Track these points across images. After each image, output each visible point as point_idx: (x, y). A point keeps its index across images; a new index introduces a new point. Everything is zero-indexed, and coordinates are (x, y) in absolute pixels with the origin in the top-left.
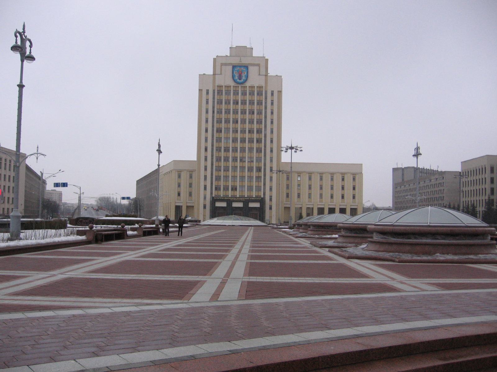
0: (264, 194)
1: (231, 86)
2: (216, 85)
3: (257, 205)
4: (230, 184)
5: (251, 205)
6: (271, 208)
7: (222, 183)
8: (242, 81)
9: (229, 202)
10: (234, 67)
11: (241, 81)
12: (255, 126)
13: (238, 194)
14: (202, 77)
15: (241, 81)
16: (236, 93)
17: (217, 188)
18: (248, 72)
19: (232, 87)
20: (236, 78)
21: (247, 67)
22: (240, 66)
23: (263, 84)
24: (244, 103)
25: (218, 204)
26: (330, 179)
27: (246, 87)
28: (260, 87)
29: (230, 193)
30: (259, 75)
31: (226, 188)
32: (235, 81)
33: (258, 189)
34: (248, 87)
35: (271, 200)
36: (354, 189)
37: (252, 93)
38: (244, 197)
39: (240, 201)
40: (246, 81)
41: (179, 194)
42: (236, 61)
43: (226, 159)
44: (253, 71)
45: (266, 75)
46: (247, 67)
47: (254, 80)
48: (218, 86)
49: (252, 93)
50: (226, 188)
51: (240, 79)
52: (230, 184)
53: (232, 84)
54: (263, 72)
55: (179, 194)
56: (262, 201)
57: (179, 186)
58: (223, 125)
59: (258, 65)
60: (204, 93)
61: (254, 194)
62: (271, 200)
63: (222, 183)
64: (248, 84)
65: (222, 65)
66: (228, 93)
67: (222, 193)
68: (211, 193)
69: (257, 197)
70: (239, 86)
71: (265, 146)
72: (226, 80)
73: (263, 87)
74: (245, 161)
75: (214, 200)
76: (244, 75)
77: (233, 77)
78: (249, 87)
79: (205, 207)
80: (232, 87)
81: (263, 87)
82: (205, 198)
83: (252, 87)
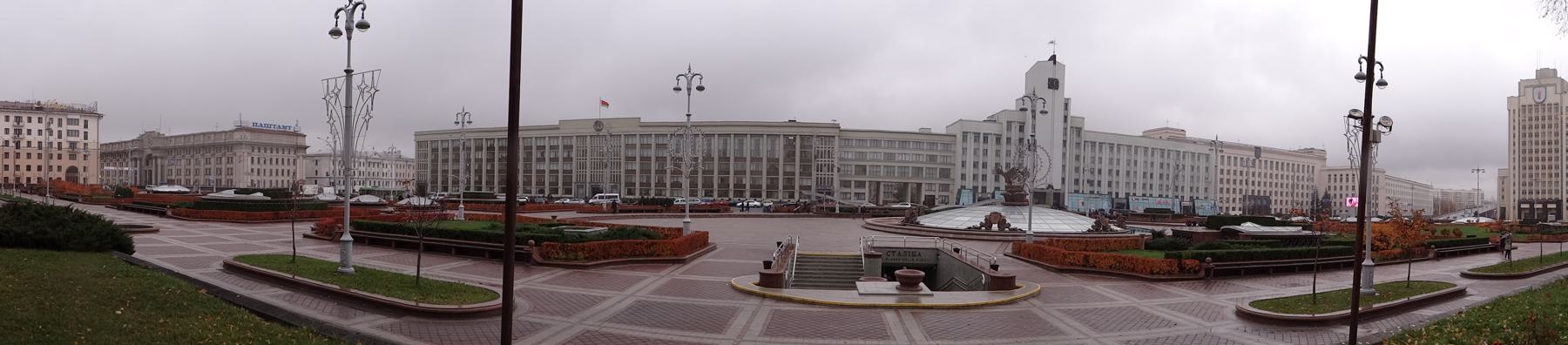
3: (1554, 206)
4: (1547, 188)
5: (1549, 206)
7: (1527, 188)
8: (1541, 100)
12: (1553, 138)
13: (1540, 196)
14: (1510, 99)
17: (1524, 193)
25: (1523, 206)
29: (1534, 196)
33: (1557, 191)
37: (1550, 110)
41: (1503, 197)
42: (1537, 83)
46: (1545, 86)
49: (1550, 110)
50: (1531, 193)
52: (1547, 188)
55: (1503, 197)
56: (1559, 202)
57: (1503, 190)
59: (1555, 85)
60: (1512, 112)
61: (1554, 196)
63: (1527, 188)
64: (1546, 102)
65: (1526, 87)
66: (1530, 111)
67: (1527, 197)
71: (1562, 155)
75: (1520, 203)
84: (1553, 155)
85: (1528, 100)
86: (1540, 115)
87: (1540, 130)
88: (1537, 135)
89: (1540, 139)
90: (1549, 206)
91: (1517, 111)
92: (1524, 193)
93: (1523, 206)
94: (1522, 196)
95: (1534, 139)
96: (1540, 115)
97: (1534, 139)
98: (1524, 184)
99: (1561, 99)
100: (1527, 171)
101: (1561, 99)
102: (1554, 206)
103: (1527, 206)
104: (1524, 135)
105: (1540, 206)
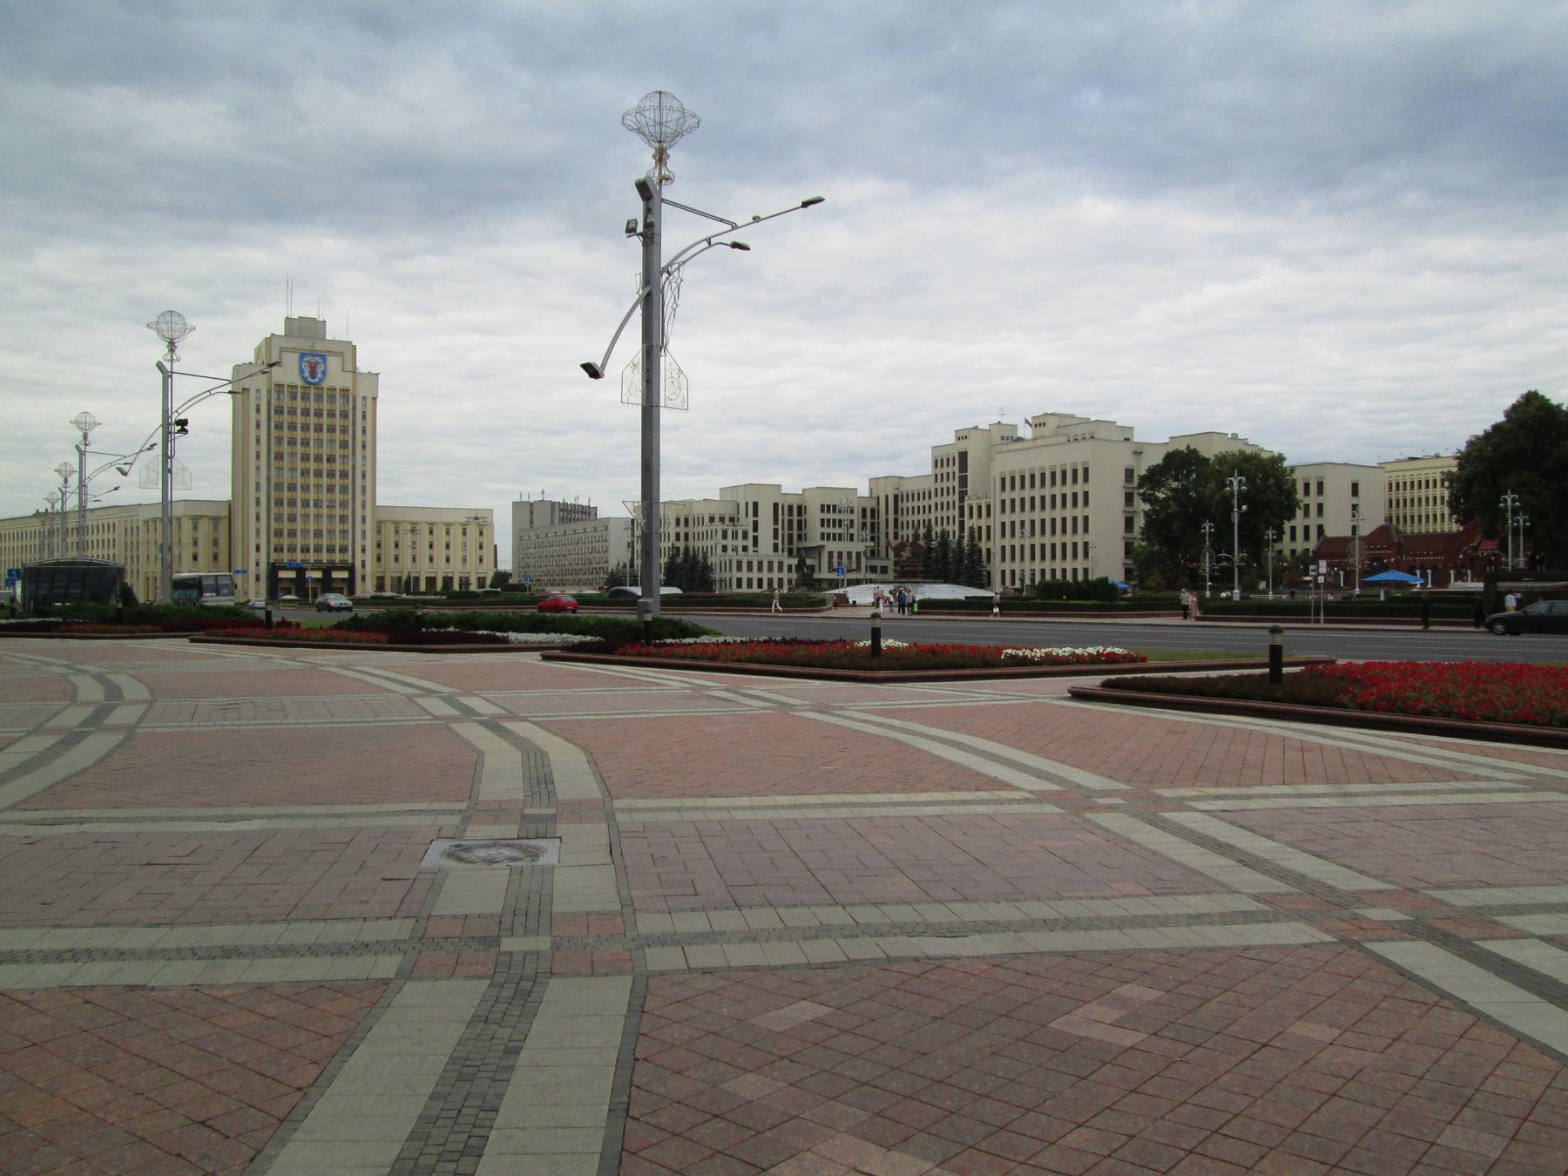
0: (353, 557)
1: (296, 387)
2: (274, 382)
3: (345, 575)
5: (336, 575)
6: (363, 578)
7: (286, 541)
8: (317, 380)
9: (301, 571)
10: (302, 356)
11: (313, 381)
13: (312, 557)
15: (313, 381)
16: (305, 397)
18: (325, 367)
19: (299, 389)
20: (307, 374)
21: (324, 357)
22: (314, 355)
23: (349, 385)
24: (319, 414)
25: (282, 574)
26: (444, 533)
27: (323, 388)
28: (345, 391)
30: (343, 371)
31: (318, 549)
32: (305, 379)
34: (325, 389)
35: (363, 565)
36: (481, 547)
38: (321, 562)
39: (318, 569)
40: (321, 380)
43: (292, 503)
44: (333, 363)
45: (354, 371)
47: (335, 377)
48: (275, 385)
49: (332, 398)
50: (292, 549)
51: (313, 374)
53: (300, 383)
54: (349, 367)
56: (351, 569)
58: (286, 449)
59: (341, 354)
61: (337, 557)
62: (363, 565)
64: (326, 384)
67: (285, 557)
68: (268, 556)
69: (341, 562)
70: (310, 388)
72: (289, 373)
73: (348, 390)
74: (321, 507)
75: (274, 569)
76: (319, 370)
77: (302, 371)
78: (328, 389)
79: (258, 578)
80: (299, 389)
81: (348, 390)
82: (258, 564)
83: (332, 389)
84: (338, 481)
85: (289, 373)
86: (312, 405)
87: (312, 435)
88: (306, 443)
89: (312, 450)
90: (336, 575)
91: (264, 393)
92: (279, 549)
93: (282, 574)
94: (274, 556)
95: (299, 449)
96: (312, 405)
97: (299, 449)
98: (279, 533)
99: (354, 382)
100: (286, 510)
101: (354, 382)
102: (345, 575)
103: (292, 574)
104: (279, 440)
105: (318, 575)
